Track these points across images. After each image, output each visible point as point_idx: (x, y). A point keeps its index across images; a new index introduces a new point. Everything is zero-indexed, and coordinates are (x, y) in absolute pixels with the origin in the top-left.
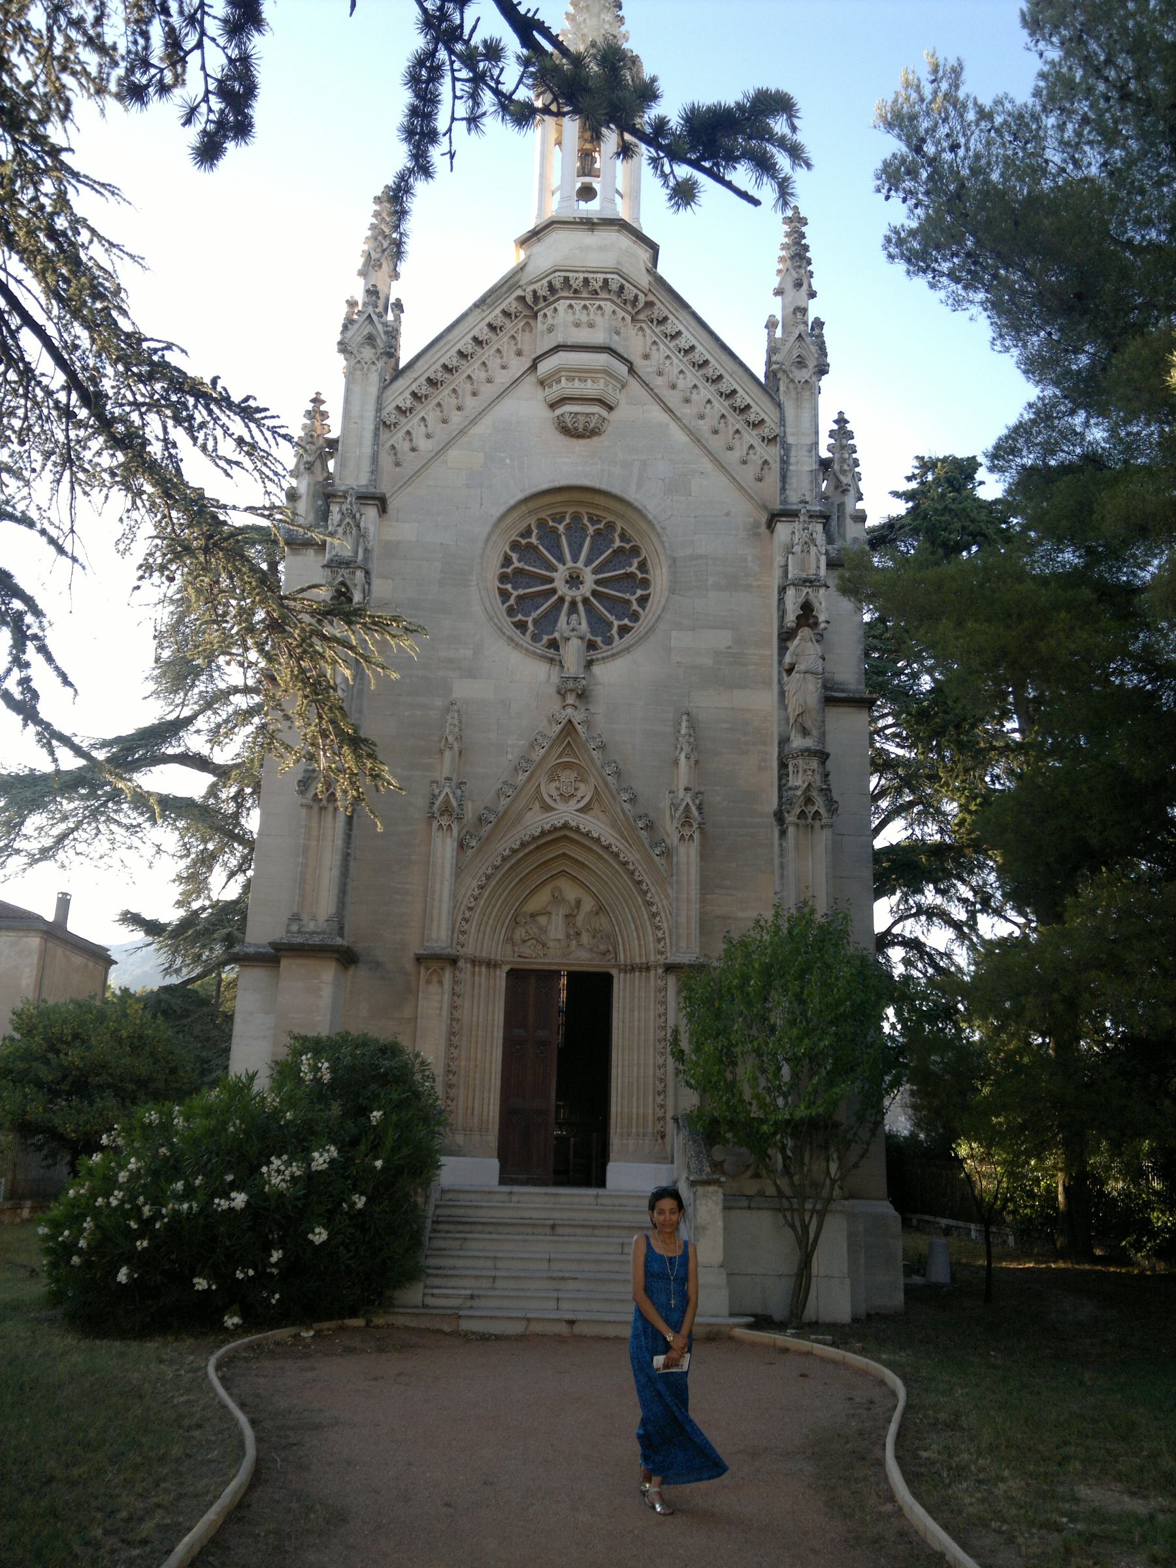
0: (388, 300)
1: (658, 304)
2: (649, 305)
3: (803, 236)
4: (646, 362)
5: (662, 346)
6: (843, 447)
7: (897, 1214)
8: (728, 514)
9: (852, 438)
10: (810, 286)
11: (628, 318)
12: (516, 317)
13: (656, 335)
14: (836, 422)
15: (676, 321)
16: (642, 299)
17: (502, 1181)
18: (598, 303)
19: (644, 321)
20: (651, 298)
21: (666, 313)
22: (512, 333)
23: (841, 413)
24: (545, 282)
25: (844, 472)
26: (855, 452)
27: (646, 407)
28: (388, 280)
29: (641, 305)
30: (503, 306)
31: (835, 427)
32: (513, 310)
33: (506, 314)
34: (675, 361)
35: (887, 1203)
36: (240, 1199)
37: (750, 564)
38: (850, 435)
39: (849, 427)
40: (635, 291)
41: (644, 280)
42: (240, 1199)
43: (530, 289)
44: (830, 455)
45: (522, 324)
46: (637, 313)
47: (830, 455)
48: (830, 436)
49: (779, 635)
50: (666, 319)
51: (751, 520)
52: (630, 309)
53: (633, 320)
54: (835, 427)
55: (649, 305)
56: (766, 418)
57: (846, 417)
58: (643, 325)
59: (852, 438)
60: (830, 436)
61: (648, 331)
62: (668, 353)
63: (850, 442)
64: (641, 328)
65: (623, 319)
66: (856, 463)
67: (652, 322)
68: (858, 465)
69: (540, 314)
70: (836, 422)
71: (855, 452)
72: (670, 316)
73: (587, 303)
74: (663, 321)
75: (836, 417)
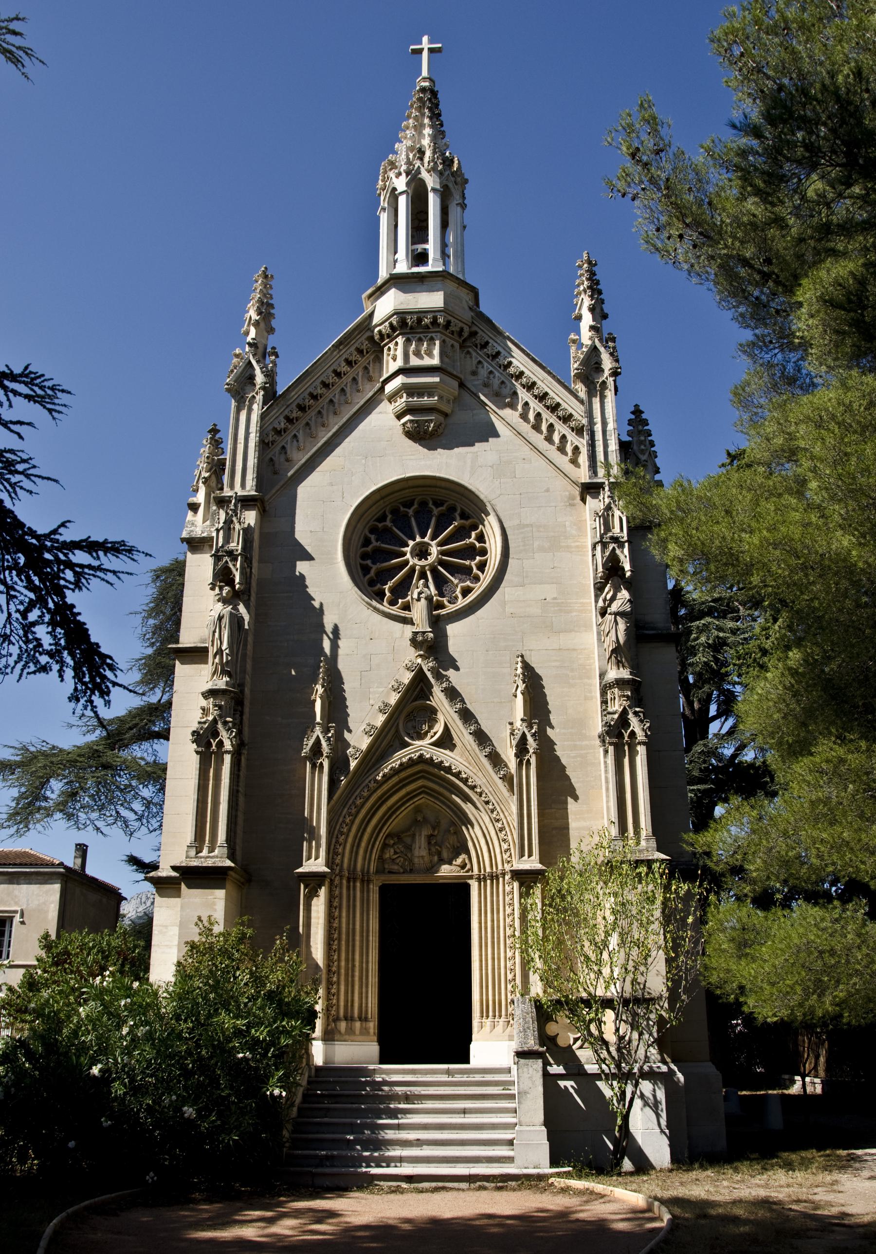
0: (266, 349)
1: (480, 333)
2: (473, 334)
3: (595, 274)
4: (473, 378)
5: (486, 364)
6: (640, 432)
7: (718, 1073)
8: (548, 490)
9: (647, 424)
10: (602, 310)
11: (457, 345)
12: (367, 352)
13: (481, 356)
14: (632, 413)
15: (495, 344)
16: (466, 330)
17: (554, 1163)
18: (430, 335)
19: (470, 347)
20: (474, 328)
21: (487, 338)
22: (365, 364)
23: (636, 406)
24: (387, 324)
25: (643, 452)
26: (650, 435)
27: (475, 412)
28: (266, 334)
29: (466, 334)
30: (356, 345)
31: (633, 417)
32: (364, 347)
33: (360, 351)
34: (497, 374)
35: (710, 1064)
36: (13, 1089)
37: (568, 529)
38: (645, 422)
39: (644, 416)
40: (461, 325)
41: (468, 316)
42: (13, 1089)
43: (377, 330)
44: (630, 439)
45: (372, 357)
46: (464, 341)
47: (630, 439)
48: (629, 424)
49: (595, 584)
50: (487, 343)
51: (567, 493)
52: (457, 338)
53: (461, 347)
54: (633, 417)
55: (473, 334)
56: (574, 413)
57: (641, 408)
58: (470, 350)
59: (647, 424)
60: (629, 424)
61: (474, 354)
62: (491, 369)
63: (646, 428)
64: (468, 352)
65: (452, 346)
66: (652, 444)
67: (476, 347)
68: (653, 446)
69: (386, 349)
70: (632, 413)
71: (650, 435)
72: (491, 341)
73: (421, 335)
74: (485, 345)
75: (633, 409)
